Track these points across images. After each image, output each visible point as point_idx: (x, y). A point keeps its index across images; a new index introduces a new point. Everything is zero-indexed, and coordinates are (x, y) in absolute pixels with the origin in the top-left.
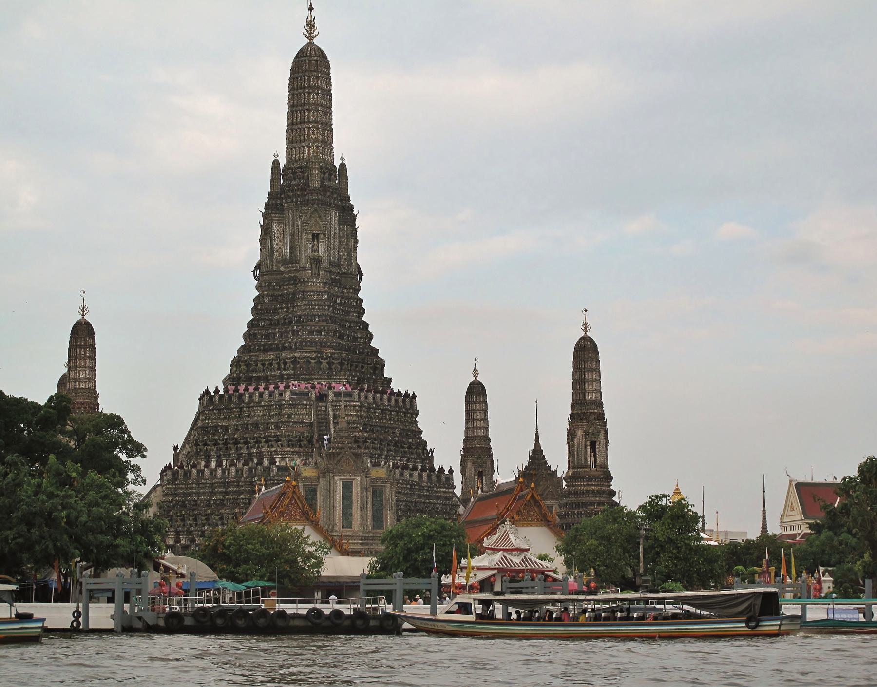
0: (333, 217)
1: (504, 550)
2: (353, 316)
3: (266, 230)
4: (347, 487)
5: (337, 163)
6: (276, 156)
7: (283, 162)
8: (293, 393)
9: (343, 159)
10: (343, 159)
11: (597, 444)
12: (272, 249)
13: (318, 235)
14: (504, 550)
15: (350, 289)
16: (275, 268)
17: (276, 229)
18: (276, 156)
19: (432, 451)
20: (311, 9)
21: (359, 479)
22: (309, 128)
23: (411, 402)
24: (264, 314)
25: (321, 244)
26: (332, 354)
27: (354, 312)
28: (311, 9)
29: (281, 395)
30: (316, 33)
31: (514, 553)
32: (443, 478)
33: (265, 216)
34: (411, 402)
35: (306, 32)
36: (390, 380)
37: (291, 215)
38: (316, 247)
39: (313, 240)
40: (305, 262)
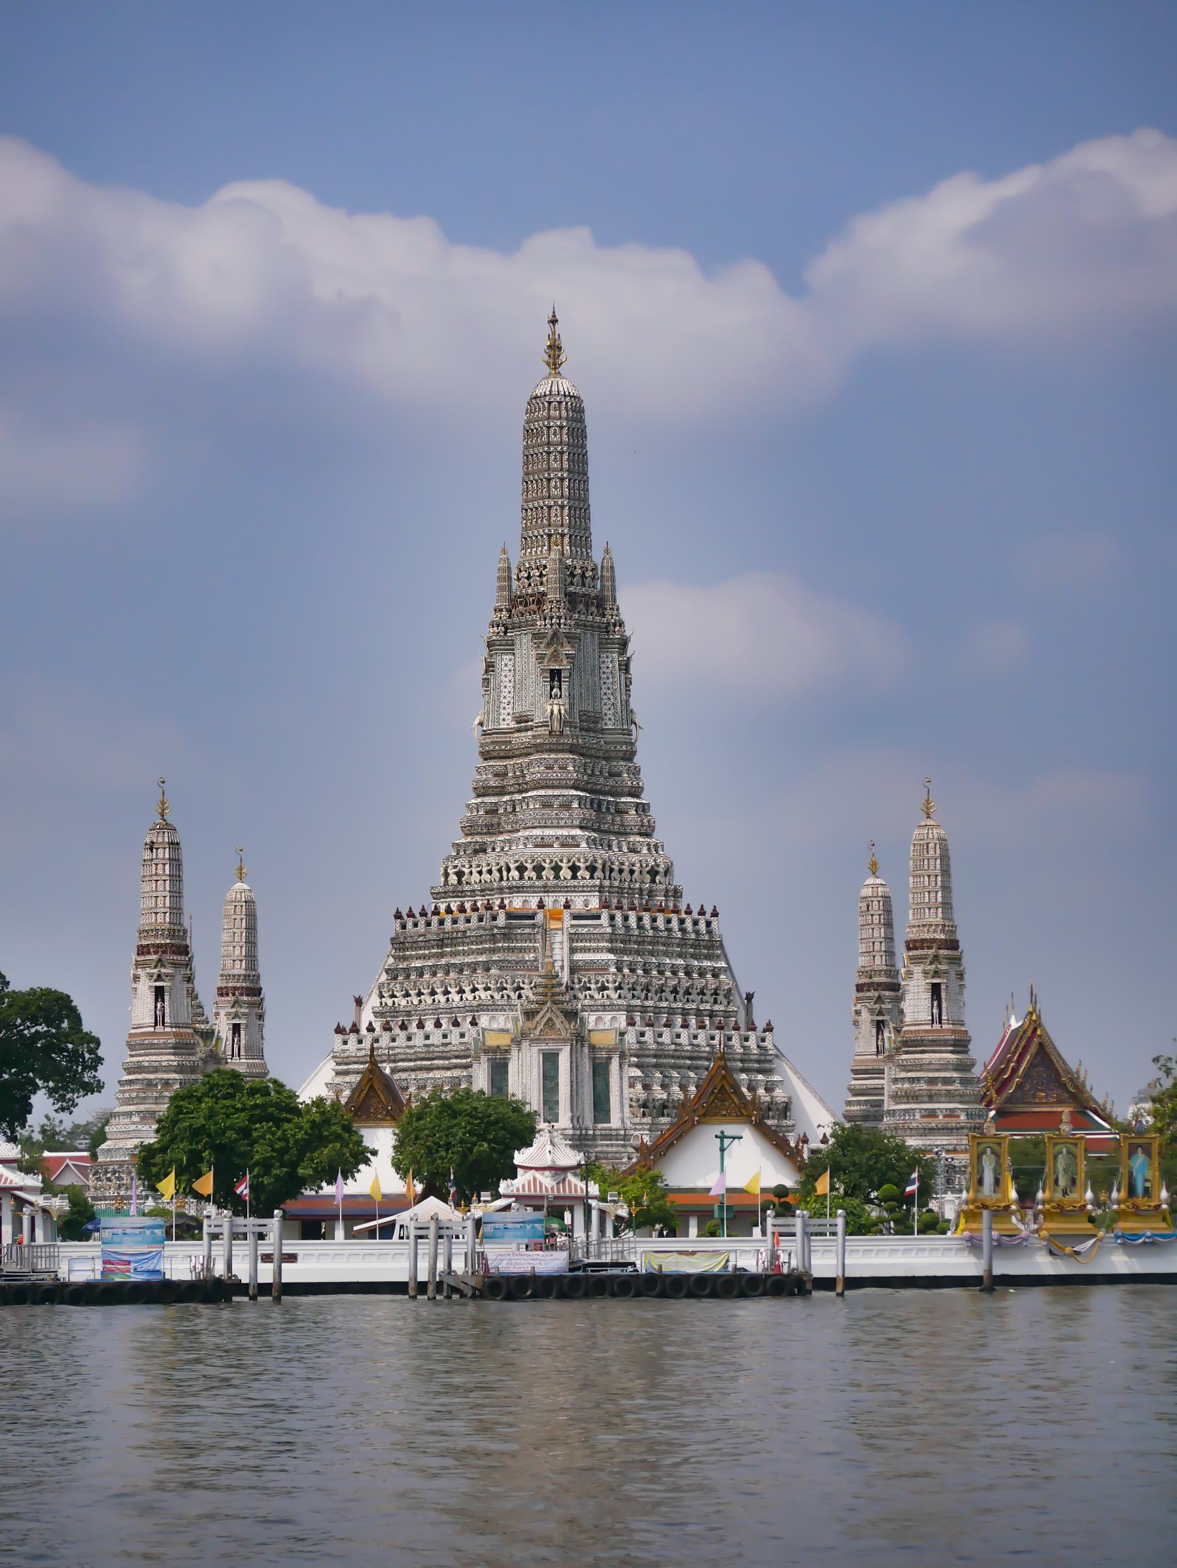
1: (537, 1169)
3: (490, 667)
4: (550, 1060)
5: (597, 555)
6: (504, 551)
8: (510, 916)
9: (607, 551)
10: (607, 551)
13: (559, 671)
14: (537, 1169)
17: (504, 662)
19: (750, 997)
21: (568, 1048)
22: (550, 507)
23: (708, 924)
28: (554, 321)
29: (494, 918)
30: (562, 358)
31: (547, 1173)
33: (490, 644)
34: (708, 924)
35: (546, 358)
37: (524, 642)
39: (552, 680)
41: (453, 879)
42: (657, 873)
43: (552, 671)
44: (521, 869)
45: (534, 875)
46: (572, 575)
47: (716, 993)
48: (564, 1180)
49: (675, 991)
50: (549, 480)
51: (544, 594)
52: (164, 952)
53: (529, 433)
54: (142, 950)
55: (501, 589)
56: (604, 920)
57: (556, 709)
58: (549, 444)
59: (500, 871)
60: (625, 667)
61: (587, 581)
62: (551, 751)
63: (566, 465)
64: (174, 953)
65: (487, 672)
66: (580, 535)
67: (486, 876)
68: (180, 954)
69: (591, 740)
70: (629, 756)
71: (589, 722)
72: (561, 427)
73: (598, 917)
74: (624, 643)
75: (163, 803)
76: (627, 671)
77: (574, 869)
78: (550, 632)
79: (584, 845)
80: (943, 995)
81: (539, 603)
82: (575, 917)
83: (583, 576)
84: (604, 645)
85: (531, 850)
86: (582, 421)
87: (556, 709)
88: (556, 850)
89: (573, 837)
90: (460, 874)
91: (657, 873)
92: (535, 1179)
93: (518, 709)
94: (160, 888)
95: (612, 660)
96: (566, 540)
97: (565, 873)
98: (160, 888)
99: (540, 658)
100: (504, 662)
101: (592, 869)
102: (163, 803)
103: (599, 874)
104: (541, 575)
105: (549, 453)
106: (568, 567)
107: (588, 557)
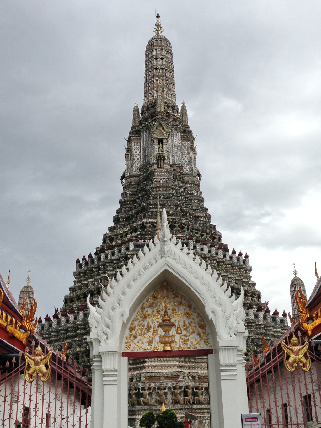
0: (176, 135)
2: (195, 203)
12: (132, 160)
15: (191, 184)
16: (134, 173)
17: (136, 147)
20: (158, 17)
22: (157, 80)
23: (244, 261)
24: (126, 204)
25: (164, 146)
26: (173, 219)
27: (195, 199)
28: (158, 17)
32: (278, 320)
38: (161, 148)
39: (159, 144)
40: (153, 160)
43: (159, 140)
76: (195, 151)
100: (136, 147)
106: (166, 103)
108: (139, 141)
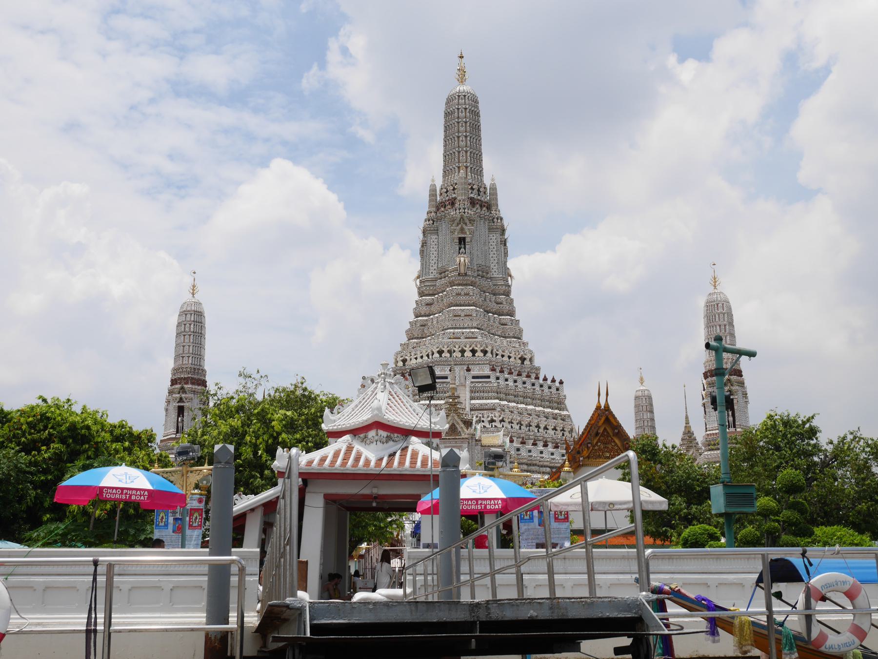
3: (424, 244)
5: (487, 181)
6: (433, 181)
7: (439, 183)
9: (493, 180)
10: (493, 180)
11: (735, 401)
13: (464, 239)
14: (356, 432)
18: (433, 181)
28: (461, 57)
31: (372, 434)
33: (424, 232)
34: (558, 389)
36: (538, 369)
37: (444, 227)
39: (460, 243)
41: (400, 364)
42: (525, 359)
44: (440, 352)
45: (448, 355)
46: (472, 189)
47: (563, 430)
48: (405, 449)
49: (538, 426)
50: (458, 137)
51: (455, 199)
52: (186, 383)
53: (447, 114)
54: (174, 382)
55: (430, 201)
56: (493, 379)
57: (462, 259)
58: (458, 118)
59: (428, 356)
60: (504, 243)
61: (481, 194)
62: (459, 285)
63: (468, 128)
64: (193, 384)
65: (422, 246)
66: (478, 171)
67: (419, 360)
68: (199, 385)
69: (484, 283)
70: (507, 294)
71: (484, 272)
72: (466, 109)
73: (488, 377)
74: (503, 231)
75: (194, 286)
76: (505, 245)
77: (474, 352)
78: (459, 216)
79: (479, 337)
80: (735, 407)
81: (453, 204)
82: (474, 377)
83: (479, 190)
84: (490, 230)
85: (446, 340)
86: (477, 107)
87: (462, 259)
88: (463, 340)
89: (473, 333)
90: (404, 361)
91: (525, 359)
92: (350, 449)
93: (440, 265)
94: (187, 341)
95: (495, 237)
96: (469, 169)
97: (468, 354)
98: (187, 341)
99: (452, 232)
101: (485, 352)
102: (194, 286)
103: (489, 355)
104: (454, 189)
105: (458, 123)
107: (482, 181)
108: (436, 231)
